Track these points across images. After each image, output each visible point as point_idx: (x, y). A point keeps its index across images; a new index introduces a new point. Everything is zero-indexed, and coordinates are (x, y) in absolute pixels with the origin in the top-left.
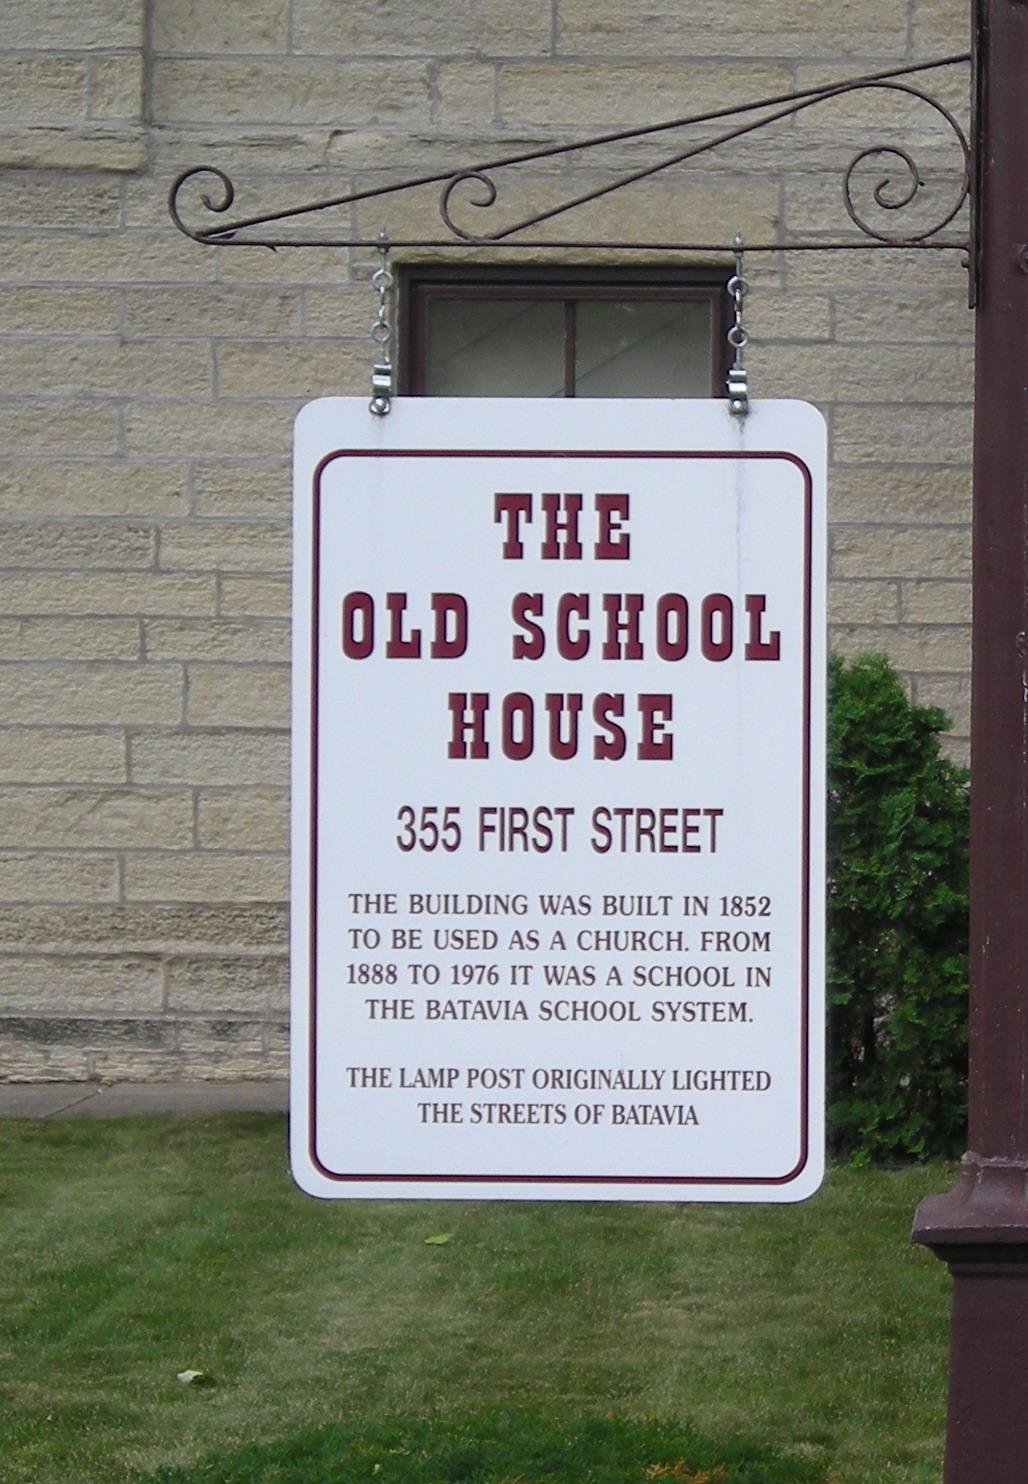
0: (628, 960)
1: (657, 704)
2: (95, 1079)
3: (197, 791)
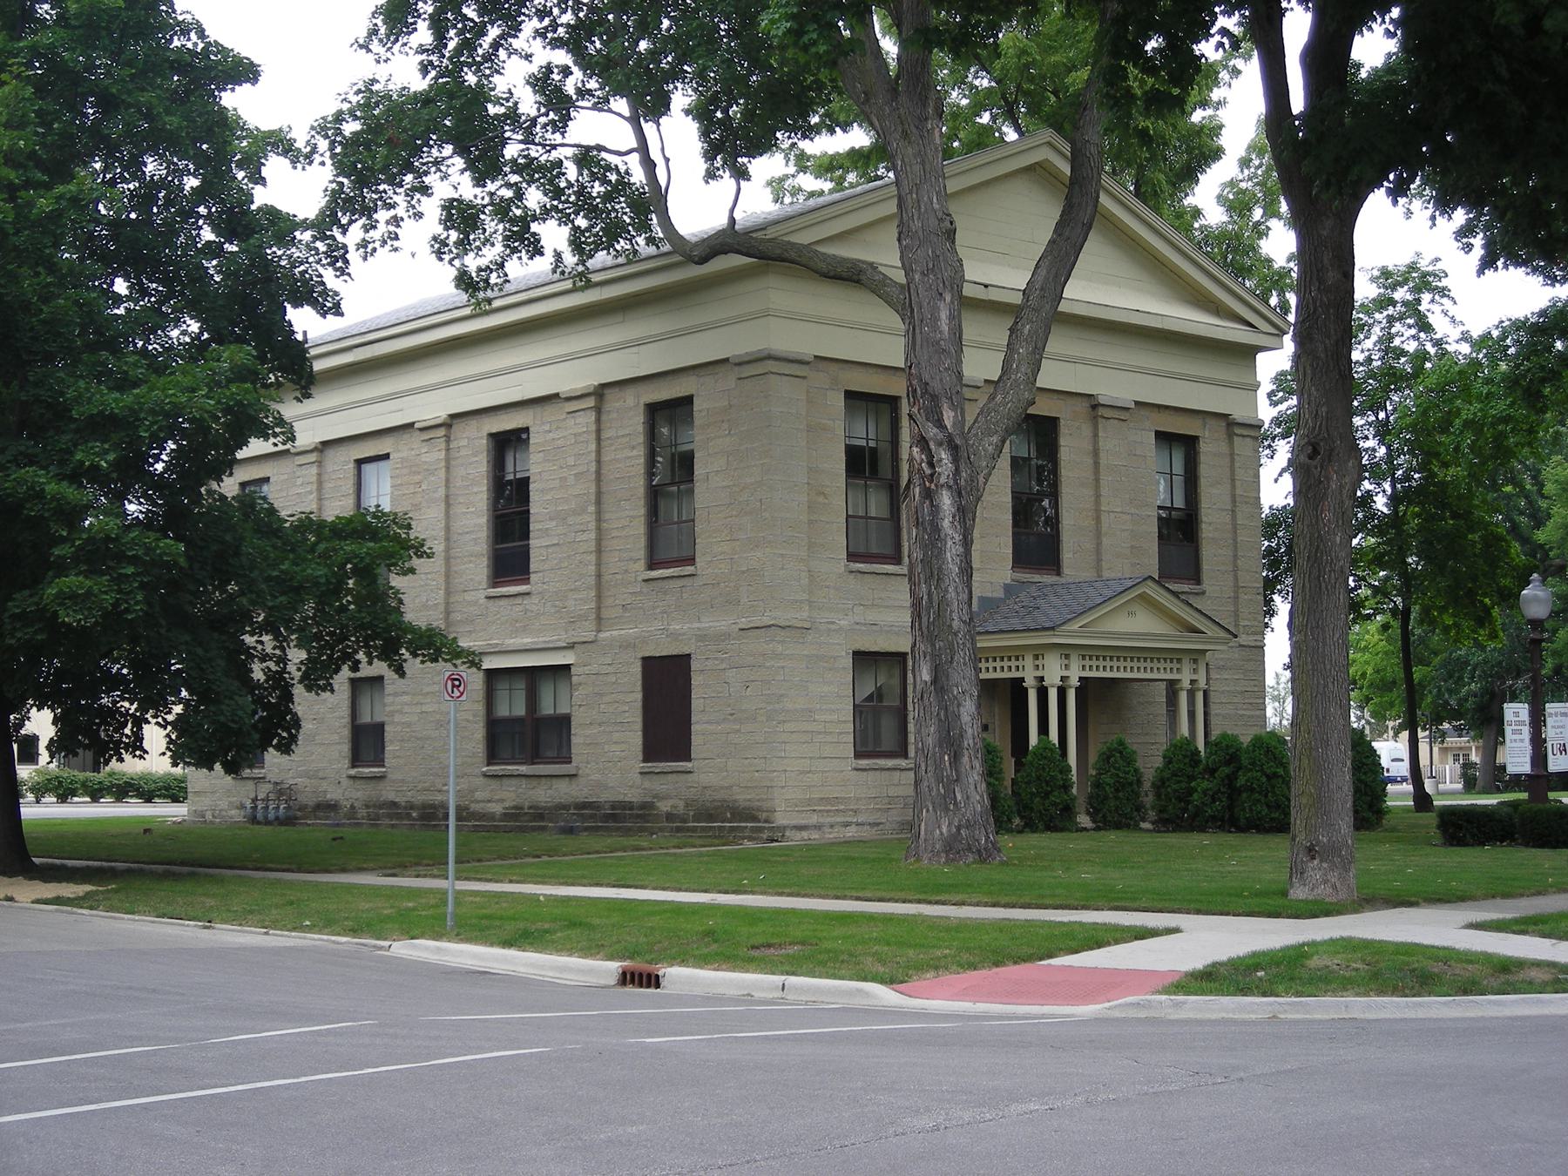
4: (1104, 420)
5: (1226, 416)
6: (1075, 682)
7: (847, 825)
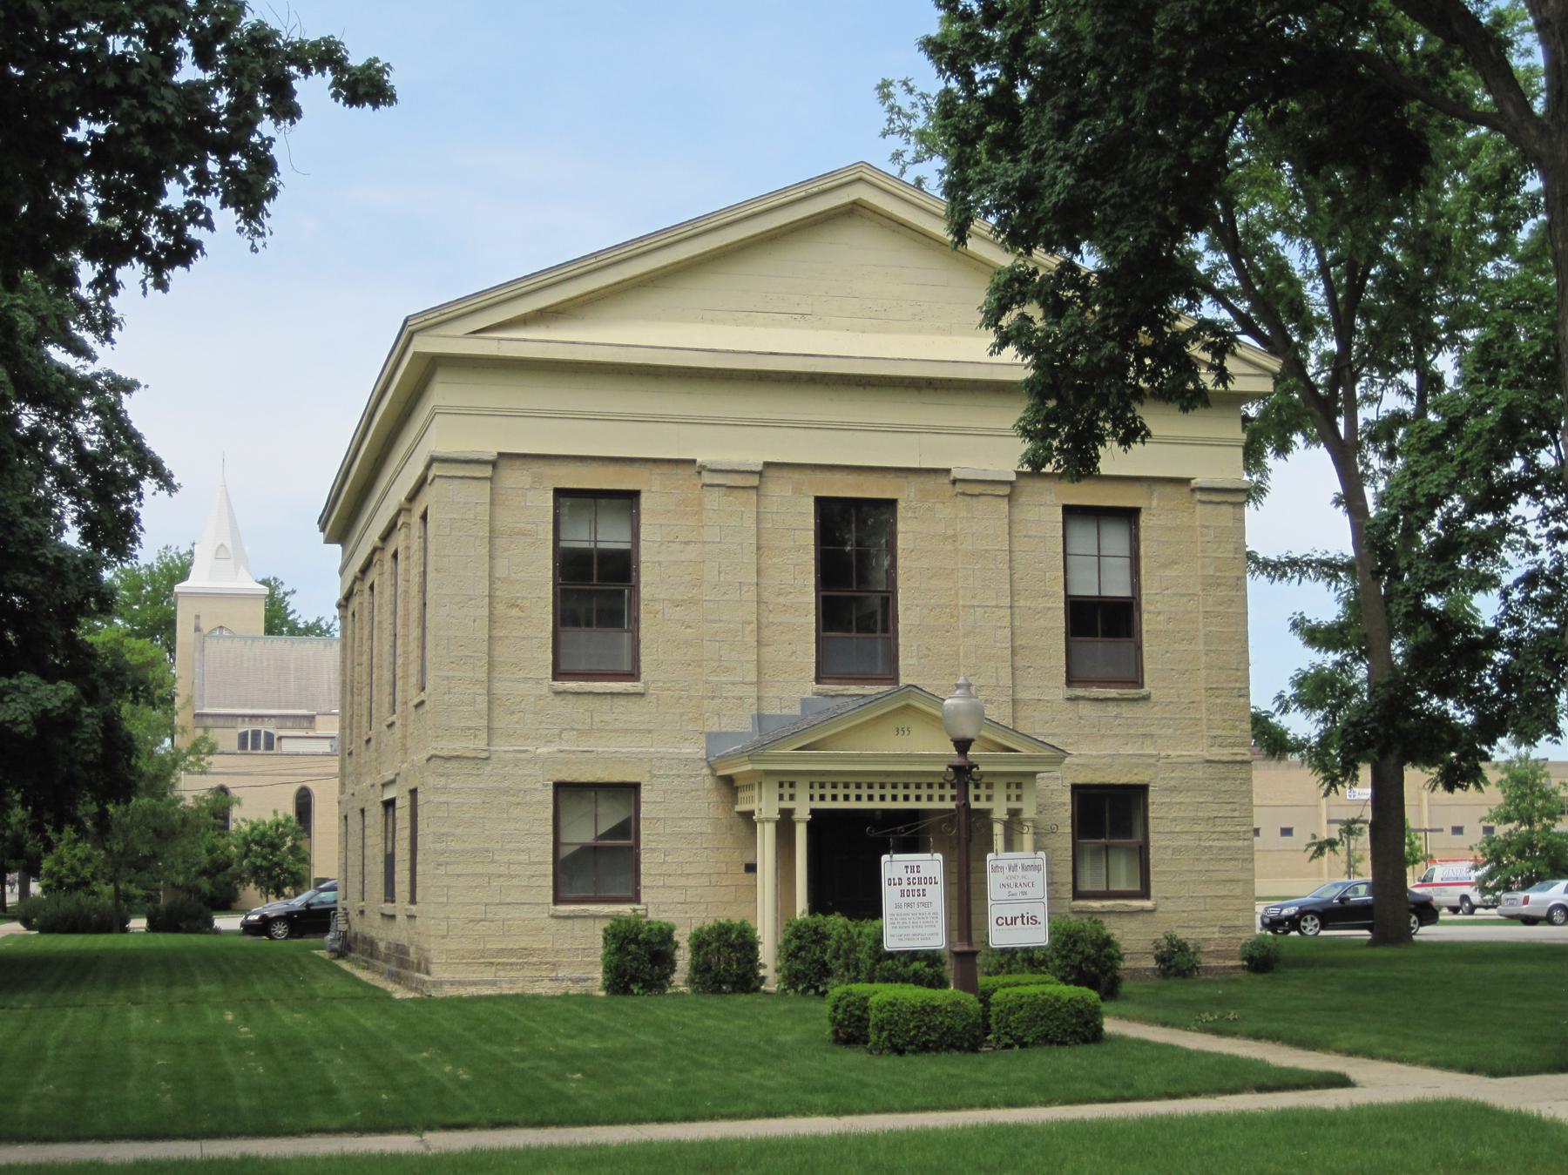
6: (802, 812)
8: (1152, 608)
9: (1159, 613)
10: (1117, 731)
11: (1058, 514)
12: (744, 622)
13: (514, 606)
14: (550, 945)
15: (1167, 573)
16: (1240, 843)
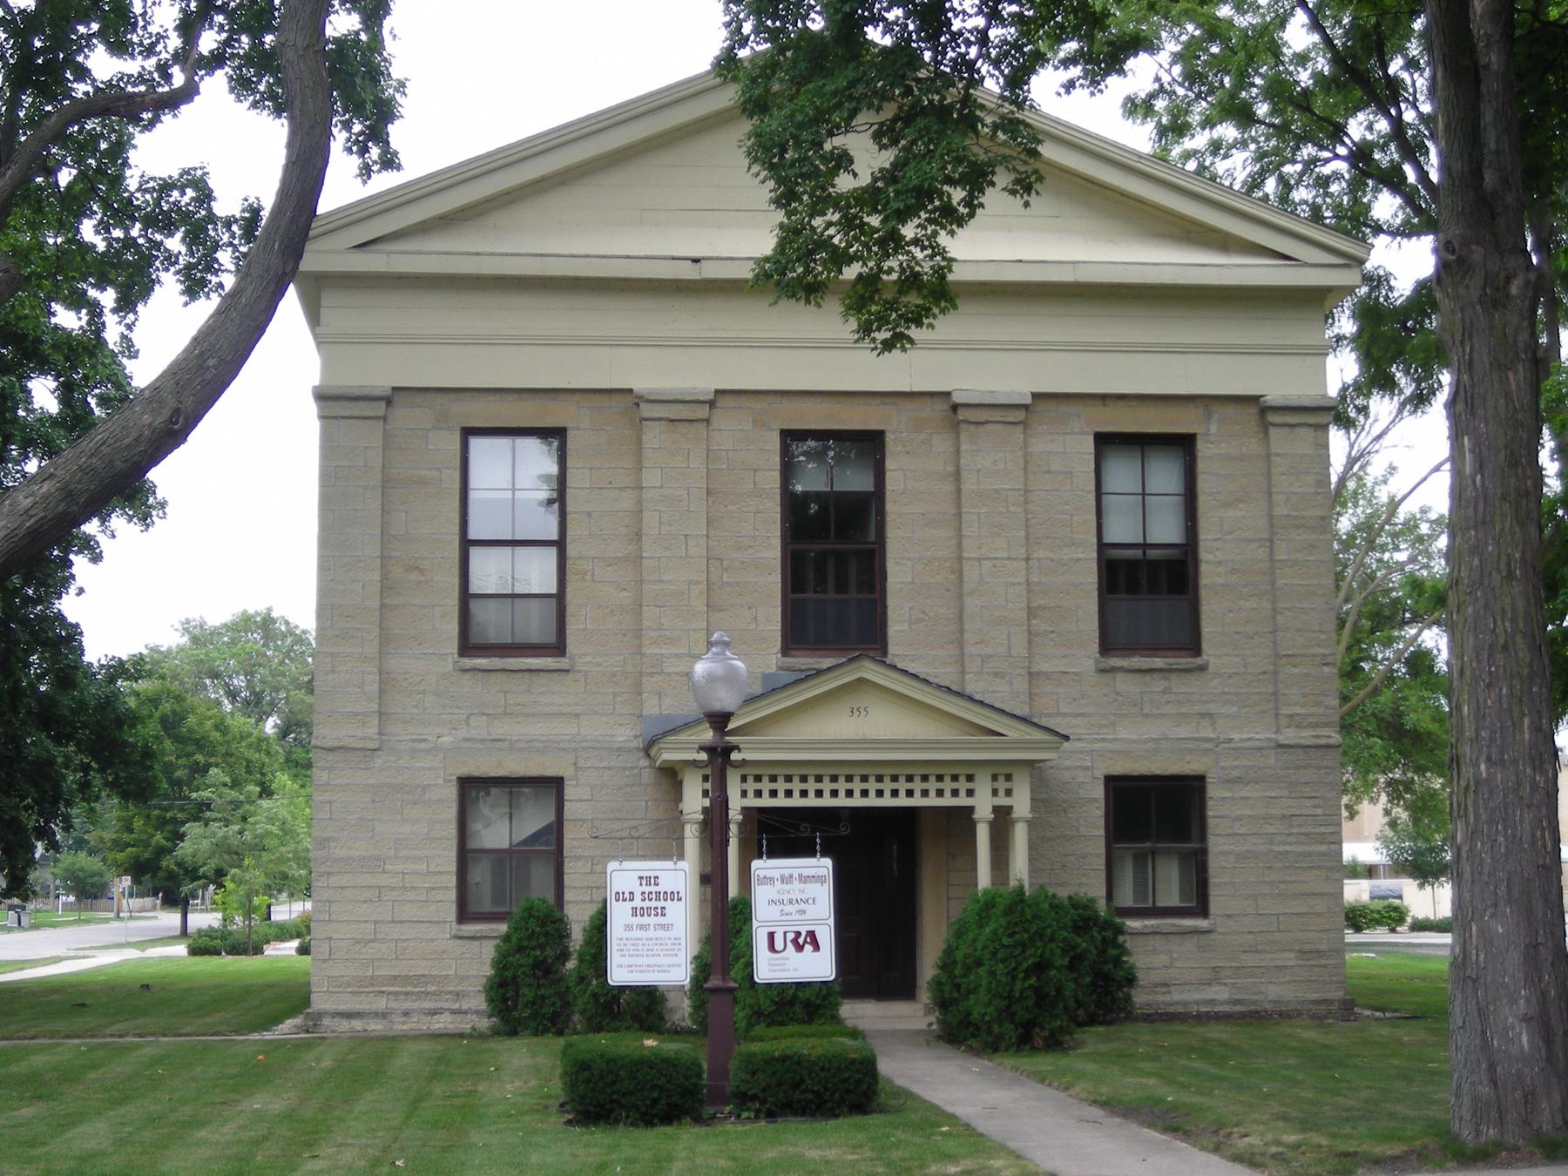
0: (659, 947)
1: (663, 908)
2: (365, 1030)
3: (397, 941)
4: (972, 428)
5: (1254, 399)
7: (433, 1013)
8: (1211, 557)
9: (1220, 563)
10: (1166, 709)
11: (1089, 445)
12: (690, 583)
13: (411, 569)
14: (452, 972)
15: (1231, 513)
16: (1324, 848)
